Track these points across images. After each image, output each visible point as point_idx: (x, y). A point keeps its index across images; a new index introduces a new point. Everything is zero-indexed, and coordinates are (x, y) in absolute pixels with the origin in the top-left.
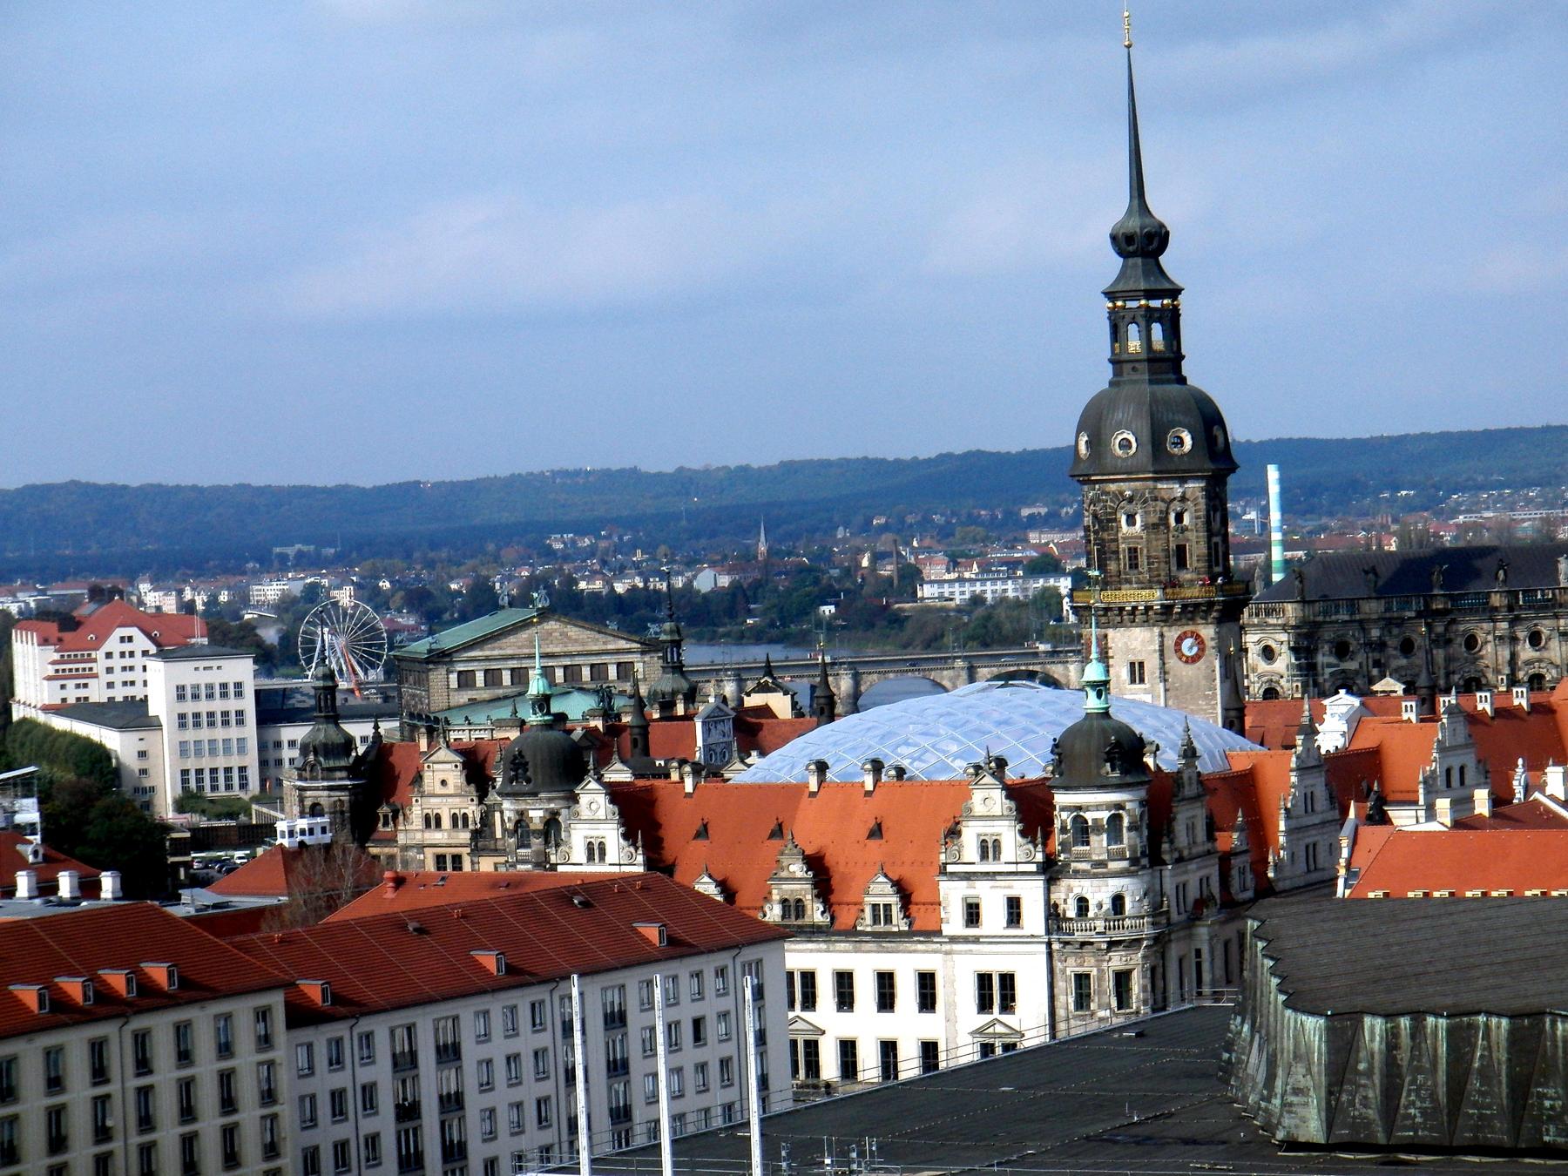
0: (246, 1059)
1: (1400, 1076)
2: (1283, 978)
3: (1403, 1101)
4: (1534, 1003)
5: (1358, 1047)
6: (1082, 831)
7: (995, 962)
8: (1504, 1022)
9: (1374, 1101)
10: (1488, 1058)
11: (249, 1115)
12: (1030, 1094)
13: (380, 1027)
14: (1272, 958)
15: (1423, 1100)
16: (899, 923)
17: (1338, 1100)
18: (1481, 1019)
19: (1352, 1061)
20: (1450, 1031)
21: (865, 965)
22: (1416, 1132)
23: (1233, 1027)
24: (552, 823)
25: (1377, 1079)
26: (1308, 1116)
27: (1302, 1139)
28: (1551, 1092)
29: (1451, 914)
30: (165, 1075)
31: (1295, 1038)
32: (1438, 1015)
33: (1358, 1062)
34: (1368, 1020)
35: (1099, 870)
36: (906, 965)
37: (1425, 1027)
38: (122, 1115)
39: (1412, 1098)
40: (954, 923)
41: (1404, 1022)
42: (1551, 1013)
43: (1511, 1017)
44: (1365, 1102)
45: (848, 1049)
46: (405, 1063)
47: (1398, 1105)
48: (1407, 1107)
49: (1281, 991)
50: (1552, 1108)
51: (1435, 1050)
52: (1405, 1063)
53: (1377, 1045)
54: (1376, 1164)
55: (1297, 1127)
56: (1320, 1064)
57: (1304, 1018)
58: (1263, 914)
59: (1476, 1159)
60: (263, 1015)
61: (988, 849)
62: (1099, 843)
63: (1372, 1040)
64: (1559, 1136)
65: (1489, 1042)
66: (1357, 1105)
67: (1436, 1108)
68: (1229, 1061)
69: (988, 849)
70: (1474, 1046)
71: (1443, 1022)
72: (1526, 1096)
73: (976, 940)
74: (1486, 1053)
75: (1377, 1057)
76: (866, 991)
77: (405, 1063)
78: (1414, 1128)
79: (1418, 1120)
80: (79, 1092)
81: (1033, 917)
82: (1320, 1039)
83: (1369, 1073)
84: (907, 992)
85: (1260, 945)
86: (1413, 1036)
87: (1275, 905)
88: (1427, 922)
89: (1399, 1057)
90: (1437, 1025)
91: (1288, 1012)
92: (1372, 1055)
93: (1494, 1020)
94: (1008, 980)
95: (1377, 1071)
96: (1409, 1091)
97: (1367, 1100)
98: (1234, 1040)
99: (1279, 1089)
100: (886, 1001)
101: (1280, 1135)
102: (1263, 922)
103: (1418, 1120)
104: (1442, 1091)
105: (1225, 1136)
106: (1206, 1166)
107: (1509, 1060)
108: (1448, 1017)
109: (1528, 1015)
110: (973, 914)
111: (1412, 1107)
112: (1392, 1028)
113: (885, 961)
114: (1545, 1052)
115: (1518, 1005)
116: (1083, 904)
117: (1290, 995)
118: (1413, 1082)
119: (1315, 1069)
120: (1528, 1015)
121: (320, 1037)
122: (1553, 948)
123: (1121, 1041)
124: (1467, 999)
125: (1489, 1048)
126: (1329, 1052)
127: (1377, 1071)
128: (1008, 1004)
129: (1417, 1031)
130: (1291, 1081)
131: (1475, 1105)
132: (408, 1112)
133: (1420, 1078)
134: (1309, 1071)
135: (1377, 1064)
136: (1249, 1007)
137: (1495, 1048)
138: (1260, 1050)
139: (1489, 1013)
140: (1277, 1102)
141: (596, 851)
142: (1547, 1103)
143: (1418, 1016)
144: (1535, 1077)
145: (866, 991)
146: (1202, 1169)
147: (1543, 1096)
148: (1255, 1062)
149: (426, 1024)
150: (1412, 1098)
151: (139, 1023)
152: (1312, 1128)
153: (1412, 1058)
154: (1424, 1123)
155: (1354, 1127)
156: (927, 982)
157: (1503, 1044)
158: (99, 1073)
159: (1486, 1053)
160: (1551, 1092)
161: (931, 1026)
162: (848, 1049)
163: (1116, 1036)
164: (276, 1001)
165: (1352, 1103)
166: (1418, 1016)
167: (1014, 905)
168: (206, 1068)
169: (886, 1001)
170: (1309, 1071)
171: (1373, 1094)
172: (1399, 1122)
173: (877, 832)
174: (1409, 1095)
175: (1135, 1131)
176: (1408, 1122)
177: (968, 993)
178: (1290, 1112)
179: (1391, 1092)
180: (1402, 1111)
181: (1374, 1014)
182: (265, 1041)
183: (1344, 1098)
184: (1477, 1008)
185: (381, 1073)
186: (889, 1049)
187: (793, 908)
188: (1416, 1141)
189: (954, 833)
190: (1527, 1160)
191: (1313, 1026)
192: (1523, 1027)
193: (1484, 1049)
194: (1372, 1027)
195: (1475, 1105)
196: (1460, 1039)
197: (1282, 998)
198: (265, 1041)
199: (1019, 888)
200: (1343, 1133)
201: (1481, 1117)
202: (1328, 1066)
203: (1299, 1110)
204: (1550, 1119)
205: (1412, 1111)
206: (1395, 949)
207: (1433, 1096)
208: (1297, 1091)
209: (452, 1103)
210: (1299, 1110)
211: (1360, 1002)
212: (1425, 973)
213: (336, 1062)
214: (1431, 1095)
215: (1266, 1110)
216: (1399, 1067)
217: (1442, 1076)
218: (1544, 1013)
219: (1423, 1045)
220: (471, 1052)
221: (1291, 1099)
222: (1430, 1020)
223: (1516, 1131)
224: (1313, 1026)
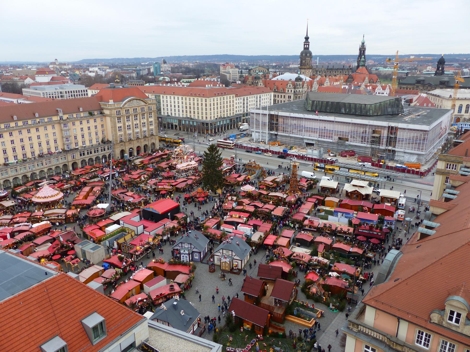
0: (232, 99)
6: (297, 85)
7: (290, 95)
11: (232, 104)
13: (242, 98)
16: (283, 91)
21: (280, 95)
24: (257, 82)
30: (225, 100)
35: (298, 88)
36: (283, 95)
38: (222, 103)
40: (287, 92)
45: (278, 101)
46: (244, 100)
60: (233, 96)
61: (290, 86)
69: (290, 86)
76: (280, 96)
77: (244, 100)
80: (219, 102)
81: (293, 92)
84: (283, 96)
94: (290, 96)
97: (314, 108)
100: (281, 97)
110: (288, 91)
113: (281, 94)
121: (237, 98)
132: (244, 104)
141: (261, 85)
145: (280, 96)
149: (245, 97)
151: (223, 96)
152: (310, 110)
156: (284, 96)
158: (221, 100)
161: (284, 99)
162: (278, 101)
164: (234, 95)
167: (291, 90)
168: (228, 100)
169: (281, 97)
182: (233, 98)
185: (242, 101)
186: (281, 101)
187: (275, 90)
198: (233, 98)
199: (292, 89)
209: (247, 103)
213: (239, 100)
220: (249, 100)
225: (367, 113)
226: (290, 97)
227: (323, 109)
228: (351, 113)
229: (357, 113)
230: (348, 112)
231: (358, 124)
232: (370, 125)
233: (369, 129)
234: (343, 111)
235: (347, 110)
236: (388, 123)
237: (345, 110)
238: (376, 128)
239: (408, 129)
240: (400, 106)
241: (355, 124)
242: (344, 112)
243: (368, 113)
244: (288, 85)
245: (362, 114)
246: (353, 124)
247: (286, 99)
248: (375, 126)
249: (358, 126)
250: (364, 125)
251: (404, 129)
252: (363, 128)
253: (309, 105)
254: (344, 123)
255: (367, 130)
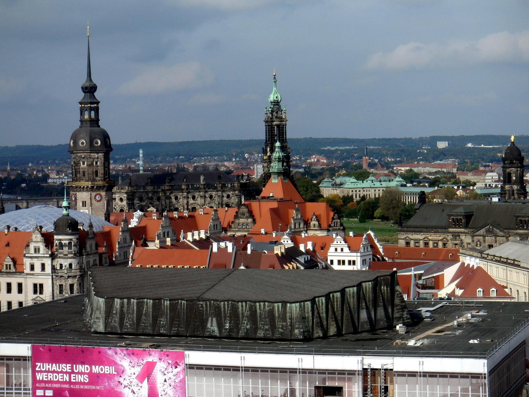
1: (124, 315)
2: (95, 288)
3: (125, 321)
4: (160, 296)
5: (113, 306)
6: (61, 246)
7: (38, 281)
8: (151, 301)
9: (117, 321)
10: (147, 311)
12: (31, 317)
14: (93, 282)
15: (130, 321)
16: (13, 269)
17: (108, 321)
18: (146, 300)
19: (112, 311)
20: (137, 303)
22: (128, 330)
23: (85, 300)
25: (118, 315)
26: (100, 325)
27: (98, 331)
28: (163, 320)
29: (142, 272)
31: (97, 303)
32: (134, 299)
33: (113, 311)
34: (116, 300)
35: (65, 257)
36: (14, 281)
37: (131, 302)
39: (127, 321)
40: (27, 270)
41: (125, 300)
42: (163, 299)
43: (153, 300)
44: (115, 322)
47: (124, 323)
48: (126, 323)
49: (94, 291)
50: (163, 324)
51: (134, 308)
52: (125, 311)
53: (118, 306)
54: (118, 338)
55: (97, 328)
56: (103, 311)
57: (99, 298)
58: (93, 270)
59: (143, 337)
61: (37, 250)
62: (66, 249)
63: (117, 305)
64: (164, 331)
65: (147, 307)
66: (113, 322)
67: (133, 324)
68: (84, 309)
69: (37, 250)
70: (143, 307)
71: (135, 301)
72: (157, 320)
73: (33, 274)
74: (147, 309)
75: (118, 310)
78: (127, 329)
79: (129, 327)
81: (48, 269)
82: (103, 304)
83: (116, 314)
84: (15, 288)
85: (91, 278)
86: (128, 304)
87: (95, 268)
88: (135, 274)
89: (124, 310)
90: (134, 301)
91: (95, 297)
92: (117, 309)
93: (149, 300)
94: (41, 286)
95: (118, 313)
96: (127, 319)
97: (115, 321)
98: (85, 304)
99: (93, 318)
101: (93, 330)
102: (92, 272)
103: (129, 327)
104: (135, 319)
105: (79, 330)
106: (72, 338)
107: (152, 311)
108: (137, 299)
109: (158, 299)
110: (32, 267)
111: (127, 323)
112: (122, 302)
114: (162, 309)
115: (155, 296)
116: (61, 266)
117: (96, 292)
118: (128, 316)
119: (102, 313)
120: (158, 299)
122: (167, 281)
123: (59, 303)
124: (142, 294)
125: (147, 308)
126: (105, 308)
127: (118, 313)
128: (41, 293)
129: (129, 303)
130: (96, 315)
131: (143, 323)
133: (129, 315)
134: (100, 313)
135: (118, 312)
136: (88, 296)
137: (149, 308)
138: (90, 307)
139: (147, 299)
140: (92, 321)
142: (162, 323)
143: (129, 299)
144: (159, 316)
146: (70, 338)
147: (161, 321)
148: (89, 309)
150: (127, 321)
152: (101, 328)
153: (127, 310)
154: (130, 327)
155: (112, 328)
156: (20, 285)
157: (151, 307)
159: (147, 309)
160: (163, 320)
161: (21, 298)
163: (59, 302)
165: (111, 322)
166: (129, 299)
167: (43, 265)
170: (100, 313)
171: (117, 319)
172: (124, 327)
173: (8, 245)
174: (126, 320)
175: (57, 327)
176: (126, 327)
177: (31, 289)
178: (95, 324)
179: (122, 319)
180: (125, 324)
181: (118, 298)
183: (110, 320)
184: (144, 297)
188: (128, 332)
189: (28, 246)
190: (156, 337)
191: (101, 300)
192: (156, 303)
193: (146, 308)
194: (117, 301)
195: (143, 323)
196: (140, 305)
197: (94, 293)
200: (109, 330)
201: (145, 326)
202: (105, 312)
203: (98, 323)
204: (162, 326)
205: (127, 324)
206: (126, 281)
207: (133, 320)
208: (97, 318)
210: (98, 323)
211: (114, 295)
212: (133, 287)
214: (132, 320)
215: (90, 323)
216: (124, 312)
217: (135, 315)
218: (162, 299)
219: (130, 307)
221: (95, 320)
222: (132, 300)
223: (154, 330)
224: (101, 300)
225: (292, 331)
226: (38, 288)
227: (147, 322)
228: (242, 333)
229: (261, 334)
230: (231, 330)
231: (264, 370)
232: (304, 371)
233: (304, 382)
234: (212, 326)
235: (227, 326)
236: (359, 358)
237: (220, 326)
238: (324, 380)
239: (425, 374)
240: (397, 301)
241: (255, 370)
242: (217, 333)
243: (296, 331)
244: (32, 246)
245: (277, 336)
246: (247, 369)
247: (26, 296)
248: (322, 372)
249: (267, 378)
250: (283, 371)
251: (412, 374)
252: (283, 380)
253: (98, 314)
254: (218, 368)
255: (297, 386)
